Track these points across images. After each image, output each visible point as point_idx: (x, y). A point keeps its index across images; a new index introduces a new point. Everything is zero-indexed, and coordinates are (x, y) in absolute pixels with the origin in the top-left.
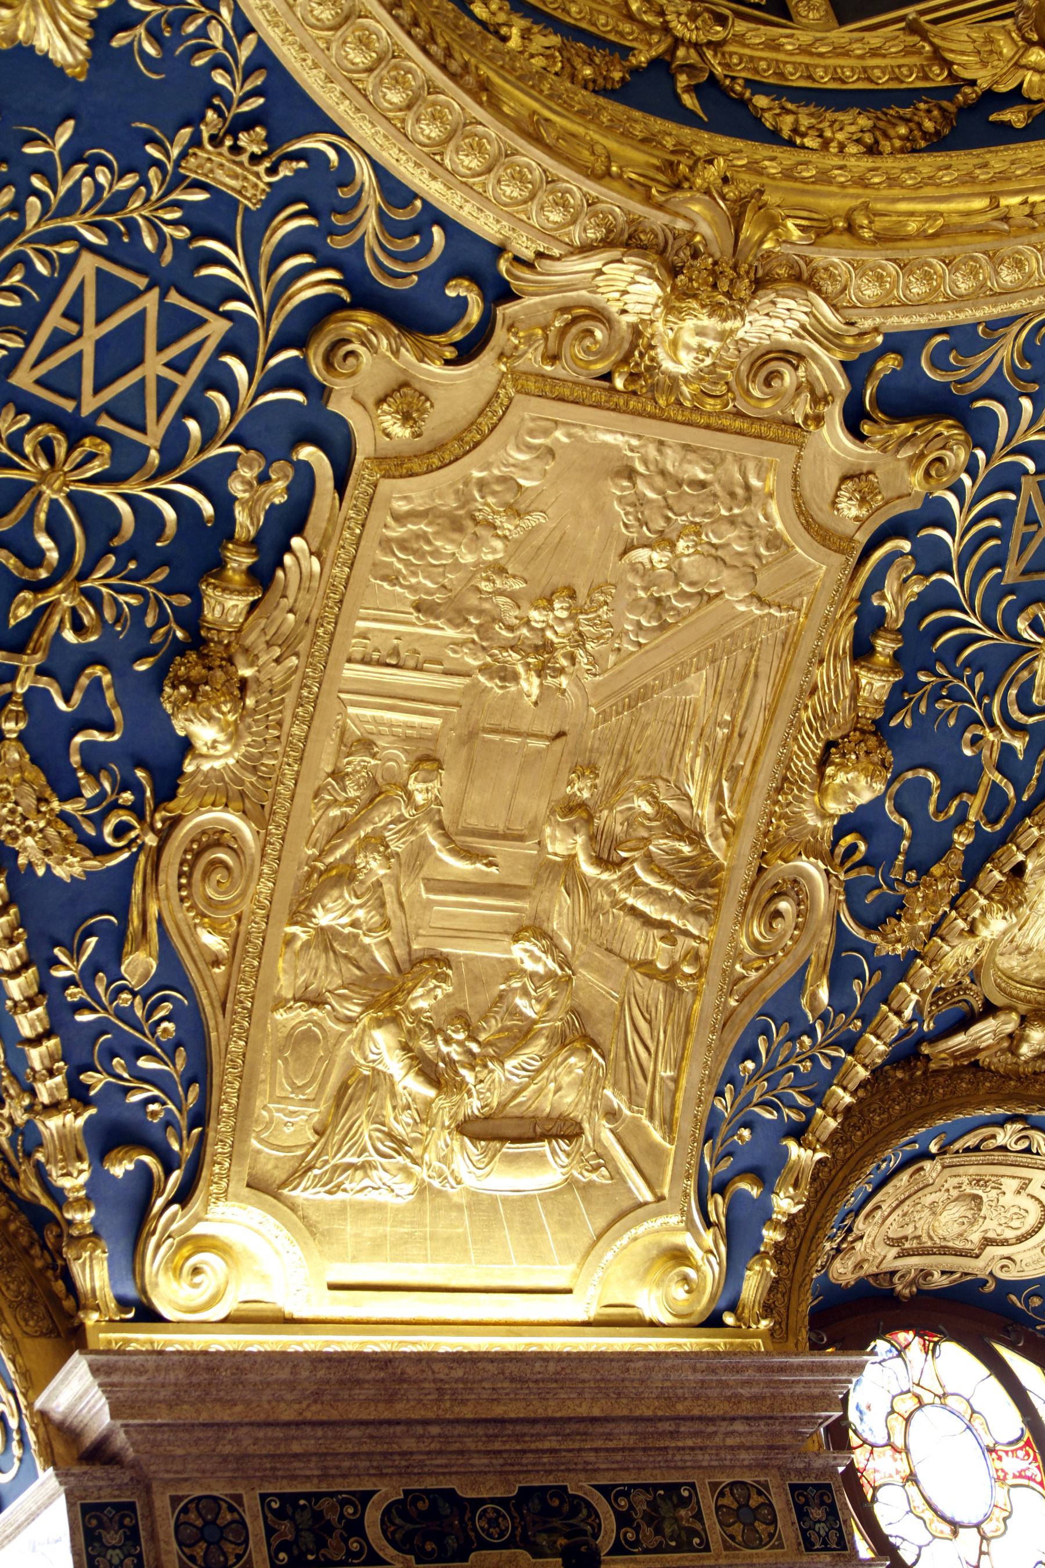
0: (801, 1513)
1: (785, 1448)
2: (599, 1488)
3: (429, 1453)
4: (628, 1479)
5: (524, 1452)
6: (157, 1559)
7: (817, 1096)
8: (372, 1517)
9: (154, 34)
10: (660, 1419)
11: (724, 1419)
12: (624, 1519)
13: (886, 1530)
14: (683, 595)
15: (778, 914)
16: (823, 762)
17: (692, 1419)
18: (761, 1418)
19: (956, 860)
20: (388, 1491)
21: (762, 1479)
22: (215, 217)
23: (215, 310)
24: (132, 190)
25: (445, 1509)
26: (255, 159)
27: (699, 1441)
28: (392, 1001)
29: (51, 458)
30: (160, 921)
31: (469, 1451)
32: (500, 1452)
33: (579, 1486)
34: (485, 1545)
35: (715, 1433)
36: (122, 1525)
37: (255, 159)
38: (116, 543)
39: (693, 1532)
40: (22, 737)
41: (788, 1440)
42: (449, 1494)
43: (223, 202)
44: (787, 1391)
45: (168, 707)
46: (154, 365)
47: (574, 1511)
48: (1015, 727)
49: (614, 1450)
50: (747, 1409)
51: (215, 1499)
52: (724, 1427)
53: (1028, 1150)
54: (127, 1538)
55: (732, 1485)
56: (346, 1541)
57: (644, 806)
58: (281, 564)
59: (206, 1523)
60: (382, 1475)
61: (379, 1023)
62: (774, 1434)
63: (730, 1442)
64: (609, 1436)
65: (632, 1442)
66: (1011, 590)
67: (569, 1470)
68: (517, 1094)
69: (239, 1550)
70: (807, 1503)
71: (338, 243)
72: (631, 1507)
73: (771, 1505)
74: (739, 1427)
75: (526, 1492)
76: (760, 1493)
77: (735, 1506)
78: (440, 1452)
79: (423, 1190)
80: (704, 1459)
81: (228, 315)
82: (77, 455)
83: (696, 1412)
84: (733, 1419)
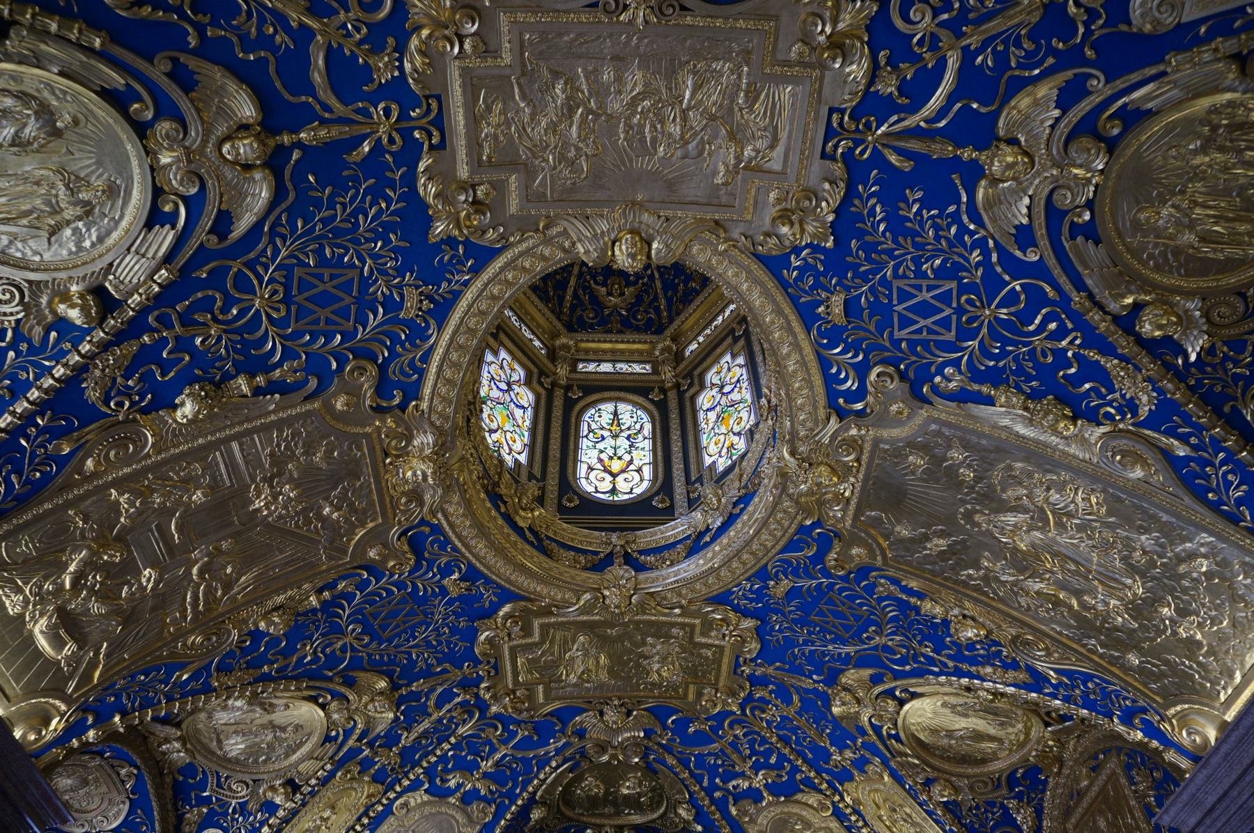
7: (142, 707)
9: (450, 260)
14: (316, 527)
15: (210, 639)
16: (276, 609)
19: (258, 672)
22: (392, 306)
23: (355, 322)
24: (389, 275)
26: (420, 309)
28: (102, 546)
29: (270, 297)
30: (87, 442)
37: (420, 309)
38: (246, 336)
40: (144, 345)
43: (400, 306)
45: (187, 392)
46: (323, 314)
48: (315, 652)
53: (123, 782)
57: (229, 571)
58: (265, 396)
61: (89, 548)
66: (363, 615)
68: (85, 615)
71: (399, 349)
79: (21, 616)
81: (356, 328)
82: (277, 305)
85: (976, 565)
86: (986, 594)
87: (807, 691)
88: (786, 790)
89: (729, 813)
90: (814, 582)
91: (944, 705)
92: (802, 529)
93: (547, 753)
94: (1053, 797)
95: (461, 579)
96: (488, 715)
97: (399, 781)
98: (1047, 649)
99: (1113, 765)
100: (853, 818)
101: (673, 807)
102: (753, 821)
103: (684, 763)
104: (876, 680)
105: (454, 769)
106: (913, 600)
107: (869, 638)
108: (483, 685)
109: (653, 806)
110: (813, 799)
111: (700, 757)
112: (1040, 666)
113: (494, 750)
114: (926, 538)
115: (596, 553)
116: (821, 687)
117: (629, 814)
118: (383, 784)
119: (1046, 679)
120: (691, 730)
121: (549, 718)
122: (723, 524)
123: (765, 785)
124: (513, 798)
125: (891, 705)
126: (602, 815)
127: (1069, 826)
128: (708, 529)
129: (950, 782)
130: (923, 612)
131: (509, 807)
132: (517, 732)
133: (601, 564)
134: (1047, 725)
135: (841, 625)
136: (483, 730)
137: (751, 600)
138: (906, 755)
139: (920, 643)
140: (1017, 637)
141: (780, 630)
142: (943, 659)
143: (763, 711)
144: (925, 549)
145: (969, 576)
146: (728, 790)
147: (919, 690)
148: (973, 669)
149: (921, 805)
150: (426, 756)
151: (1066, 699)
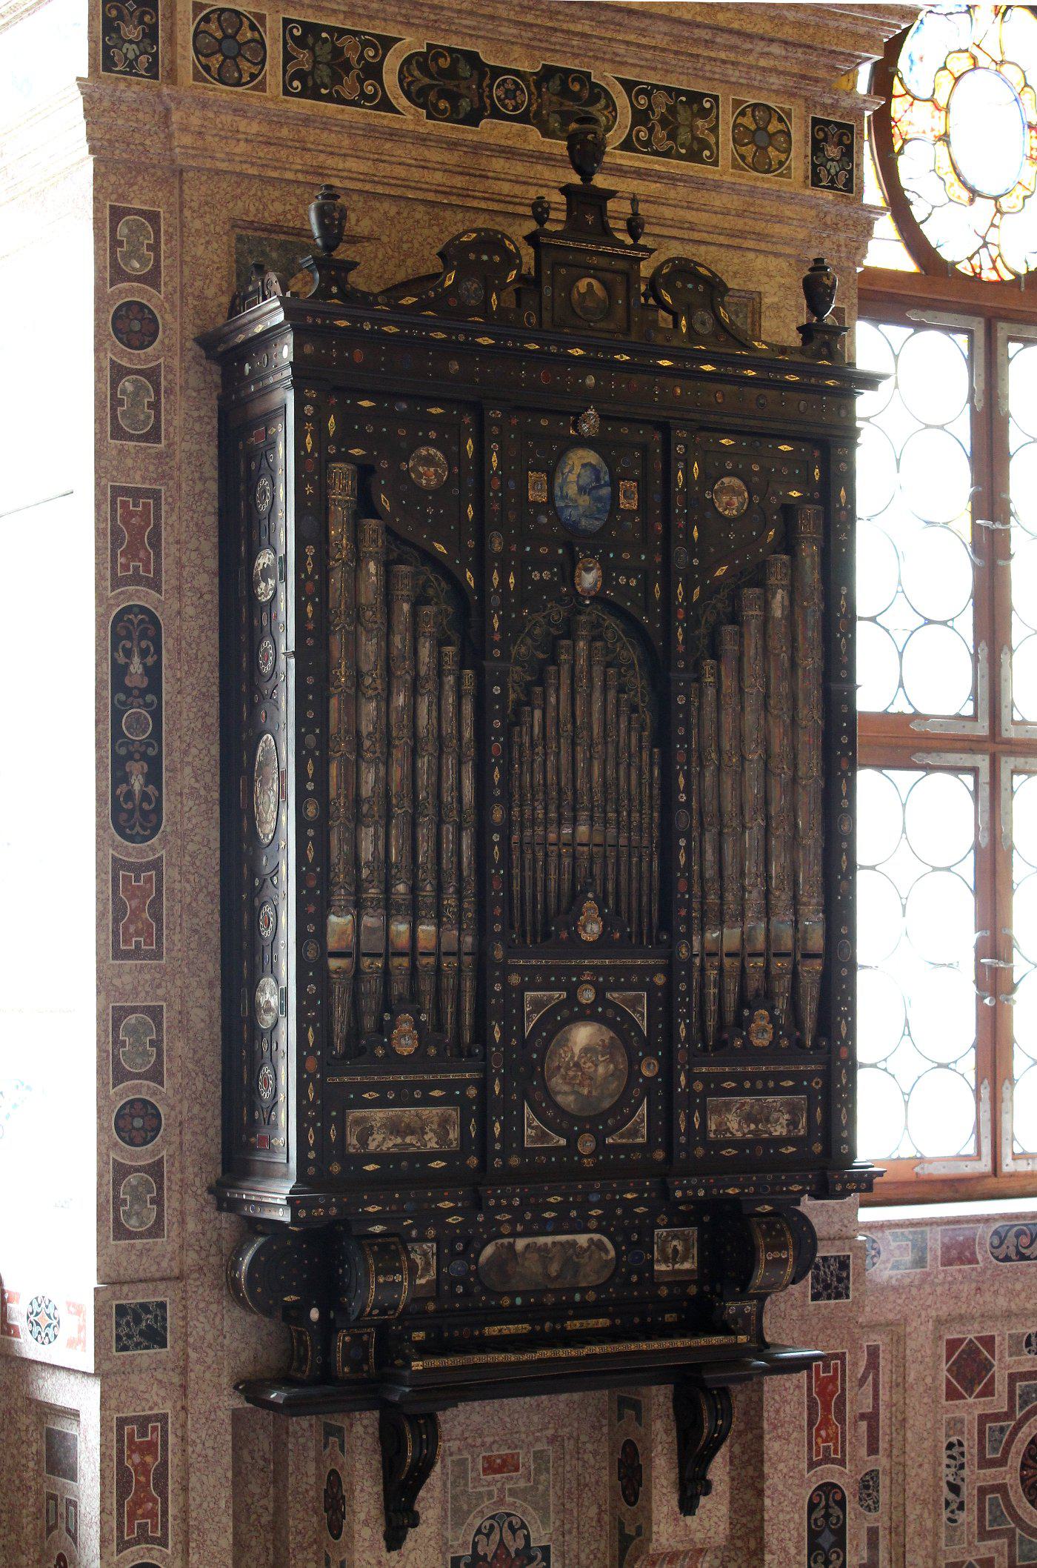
0: (817, 147)
1: (817, 80)
2: (623, 82)
3: (460, 11)
4: (653, 78)
5: (555, 30)
6: (173, 62)
8: (392, 64)
10: (698, 26)
11: (762, 39)
12: (640, 117)
13: (904, 183)
17: (731, 31)
18: (800, 46)
20: (412, 42)
21: (787, 107)
25: (464, 70)
27: (732, 56)
31: (500, 18)
32: (531, 25)
33: (604, 75)
34: (497, 114)
35: (751, 51)
36: (141, 22)
39: (704, 145)
41: (821, 73)
42: (472, 57)
44: (832, 24)
47: (594, 99)
49: (644, 47)
50: (788, 33)
51: (238, 13)
52: (760, 46)
54: (145, 35)
55: (755, 106)
56: (361, 82)
59: (226, 36)
60: (409, 24)
62: (808, 63)
63: (763, 63)
64: (643, 32)
65: (661, 41)
67: (597, 58)
69: (255, 70)
70: (825, 140)
72: (650, 107)
73: (788, 134)
74: (776, 49)
75: (549, 72)
76: (781, 120)
77: (753, 127)
78: (471, 13)
80: (734, 75)
83: (736, 26)
84: (772, 40)
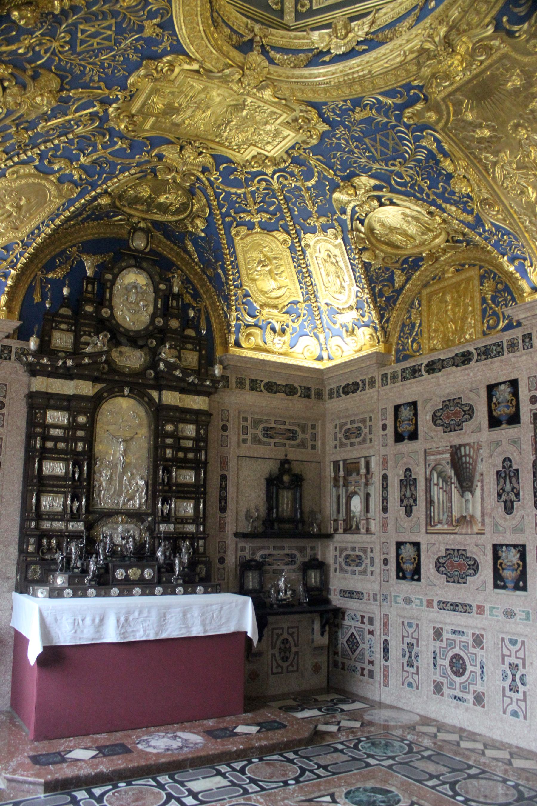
85: (496, 153)
86: (487, 171)
87: (325, 178)
88: (268, 228)
89: (230, 232)
90: (385, 120)
91: (403, 214)
92: (408, 87)
93: (130, 164)
94: (420, 275)
95: (159, 26)
96: (105, 127)
97: (18, 154)
98: (498, 211)
99: (474, 273)
100: (300, 253)
101: (193, 217)
102: (242, 239)
103: (217, 195)
104: (376, 188)
105: (61, 157)
106: (440, 157)
107: (393, 165)
108: (114, 105)
109: (178, 212)
110: (282, 236)
111: (229, 194)
112: (483, 217)
113: (95, 150)
114: (480, 126)
115: (242, 36)
116: (337, 180)
117: (156, 213)
118: (7, 154)
119: (483, 226)
120: (232, 177)
121: (145, 140)
122: (344, 53)
123: (259, 222)
124: (94, 186)
125: (376, 203)
126: (137, 210)
127: (425, 292)
128: (329, 52)
129: (374, 251)
130: (441, 165)
131: (89, 193)
132: (116, 143)
133: (245, 47)
134: (447, 241)
135: (381, 151)
136: (94, 135)
137: (335, 114)
138: (360, 232)
139: (423, 179)
140: (487, 199)
141: (339, 139)
142: (430, 193)
143: (286, 179)
144: (474, 131)
145: (486, 158)
146: (235, 219)
147: (398, 202)
148: (444, 205)
149: (350, 259)
150: (45, 142)
151: (486, 239)
